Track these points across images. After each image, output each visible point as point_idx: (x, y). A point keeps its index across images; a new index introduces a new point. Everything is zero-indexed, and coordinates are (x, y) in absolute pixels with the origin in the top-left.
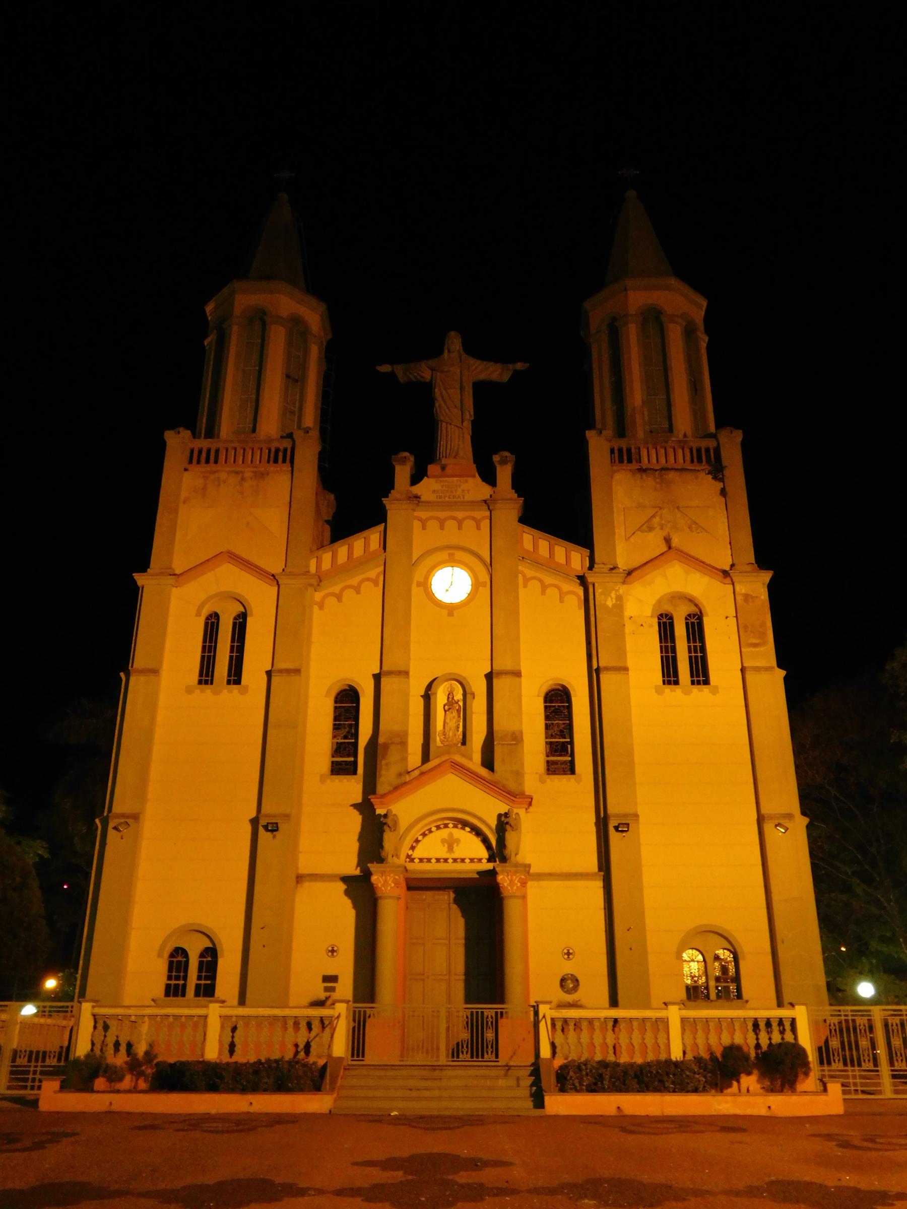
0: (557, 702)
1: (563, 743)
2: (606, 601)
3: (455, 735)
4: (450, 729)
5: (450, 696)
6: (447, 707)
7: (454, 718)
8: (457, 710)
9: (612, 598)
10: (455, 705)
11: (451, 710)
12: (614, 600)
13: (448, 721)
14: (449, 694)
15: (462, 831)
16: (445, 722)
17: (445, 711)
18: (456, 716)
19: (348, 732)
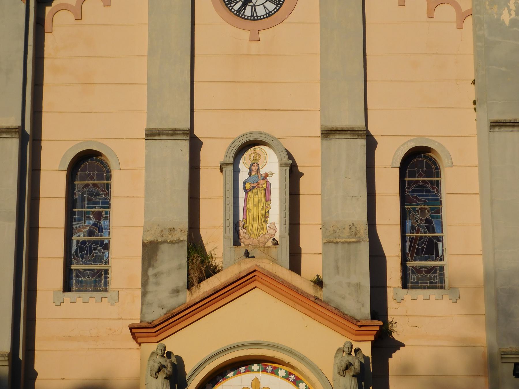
0: (421, 176)
1: (430, 239)
2: (501, 14)
3: (262, 229)
4: (254, 220)
5: (254, 168)
6: (248, 186)
7: (260, 201)
8: (265, 190)
9: (510, 11)
10: (262, 182)
11: (255, 190)
12: (513, 13)
13: (250, 206)
14: (251, 165)
15: (273, 377)
16: (245, 207)
17: (246, 192)
18: (263, 200)
19: (95, 225)
